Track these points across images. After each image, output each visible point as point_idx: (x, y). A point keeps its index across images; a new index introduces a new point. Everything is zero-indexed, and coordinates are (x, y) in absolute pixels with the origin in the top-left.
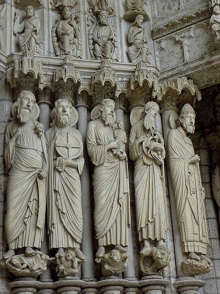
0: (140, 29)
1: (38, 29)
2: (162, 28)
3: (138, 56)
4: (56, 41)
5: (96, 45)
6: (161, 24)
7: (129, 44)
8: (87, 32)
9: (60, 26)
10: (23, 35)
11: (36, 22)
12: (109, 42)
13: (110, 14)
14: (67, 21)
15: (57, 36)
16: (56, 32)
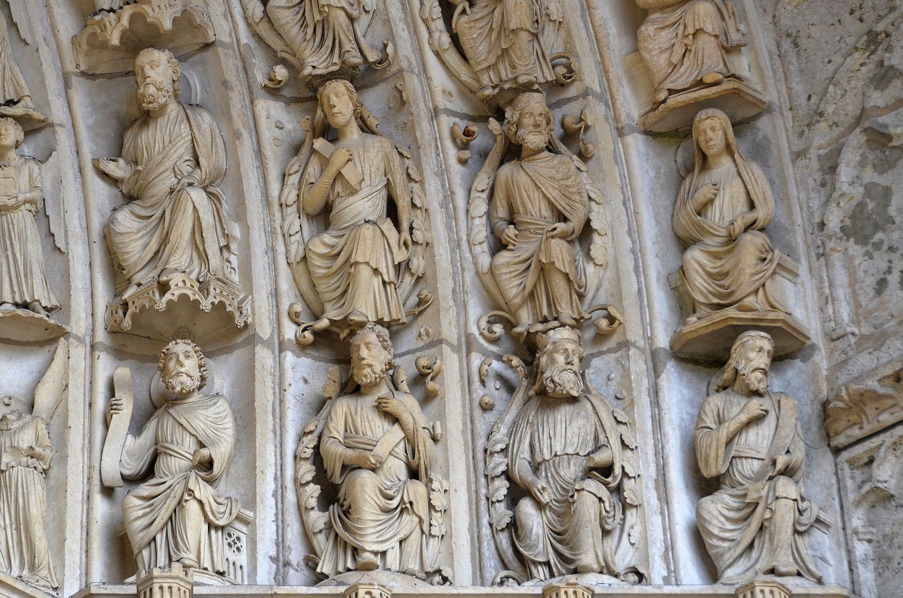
0: (755, 406)
1: (220, 452)
2: (875, 392)
3: (751, 546)
4: (313, 502)
5: (526, 506)
6: (871, 367)
7: (704, 485)
8: (481, 443)
9: (337, 428)
10: (145, 489)
11: (210, 421)
12: (592, 485)
13: (601, 337)
14: (369, 401)
15: (321, 476)
16: (318, 457)
